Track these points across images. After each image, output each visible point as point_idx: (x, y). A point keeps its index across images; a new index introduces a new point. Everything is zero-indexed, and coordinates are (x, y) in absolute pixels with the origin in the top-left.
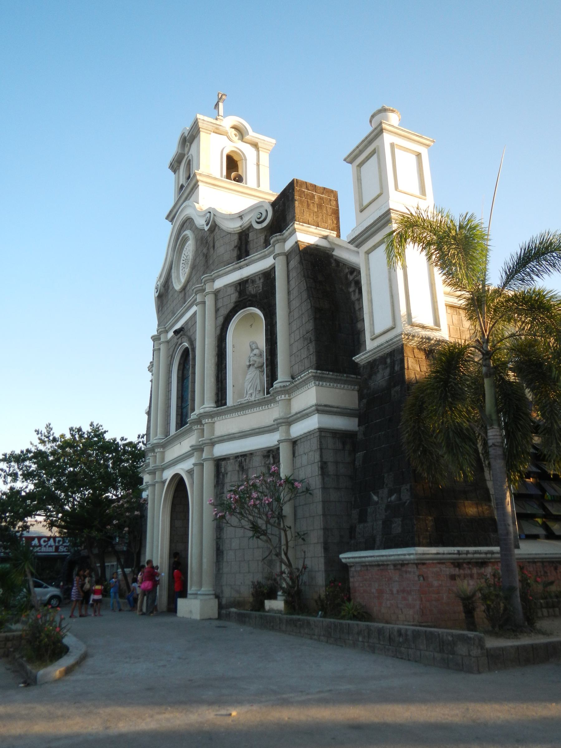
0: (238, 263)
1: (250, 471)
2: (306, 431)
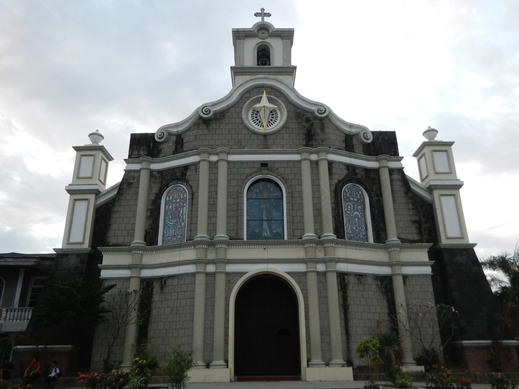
0: (350, 154)
1: (366, 286)
2: (417, 273)
